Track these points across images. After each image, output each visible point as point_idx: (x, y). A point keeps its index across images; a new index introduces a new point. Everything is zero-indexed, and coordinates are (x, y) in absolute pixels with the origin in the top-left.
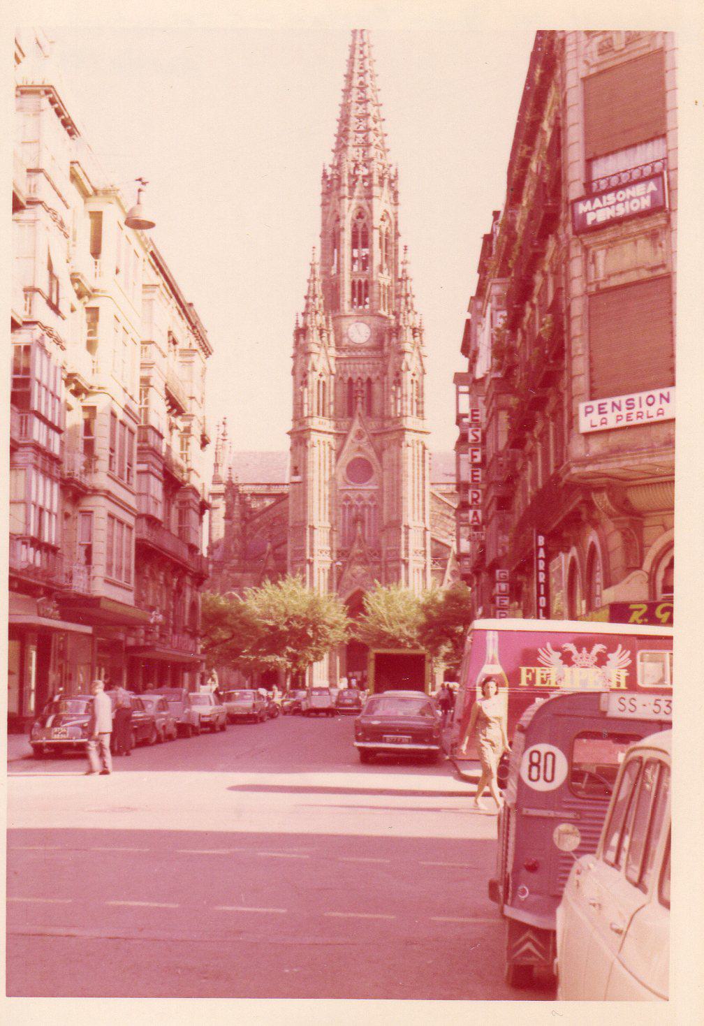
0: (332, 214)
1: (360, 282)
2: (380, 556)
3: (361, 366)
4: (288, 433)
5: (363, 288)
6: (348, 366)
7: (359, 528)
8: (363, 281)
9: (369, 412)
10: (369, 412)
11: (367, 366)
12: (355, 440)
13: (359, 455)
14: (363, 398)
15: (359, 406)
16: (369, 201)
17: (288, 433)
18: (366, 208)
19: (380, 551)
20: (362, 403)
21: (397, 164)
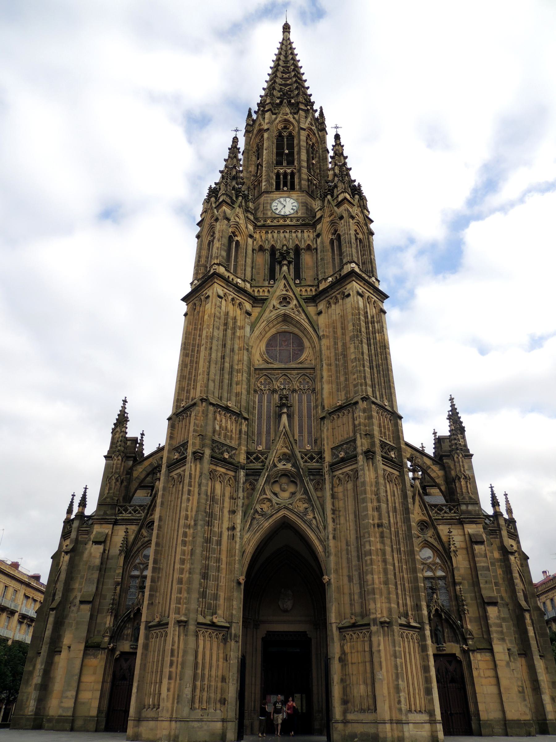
0: (256, 135)
1: (285, 172)
2: (321, 458)
3: (287, 235)
4: (184, 299)
5: (289, 177)
6: (270, 236)
7: (284, 418)
8: (289, 171)
9: (297, 275)
10: (297, 275)
11: (294, 235)
12: (278, 306)
13: (285, 328)
14: (290, 262)
15: (285, 268)
16: (295, 116)
17: (184, 299)
18: (292, 120)
19: (320, 453)
20: (289, 269)
21: (321, 108)
